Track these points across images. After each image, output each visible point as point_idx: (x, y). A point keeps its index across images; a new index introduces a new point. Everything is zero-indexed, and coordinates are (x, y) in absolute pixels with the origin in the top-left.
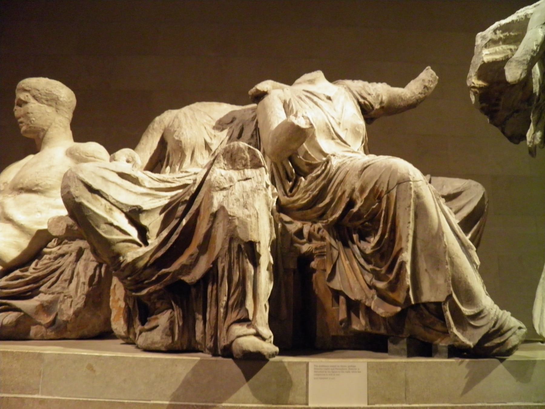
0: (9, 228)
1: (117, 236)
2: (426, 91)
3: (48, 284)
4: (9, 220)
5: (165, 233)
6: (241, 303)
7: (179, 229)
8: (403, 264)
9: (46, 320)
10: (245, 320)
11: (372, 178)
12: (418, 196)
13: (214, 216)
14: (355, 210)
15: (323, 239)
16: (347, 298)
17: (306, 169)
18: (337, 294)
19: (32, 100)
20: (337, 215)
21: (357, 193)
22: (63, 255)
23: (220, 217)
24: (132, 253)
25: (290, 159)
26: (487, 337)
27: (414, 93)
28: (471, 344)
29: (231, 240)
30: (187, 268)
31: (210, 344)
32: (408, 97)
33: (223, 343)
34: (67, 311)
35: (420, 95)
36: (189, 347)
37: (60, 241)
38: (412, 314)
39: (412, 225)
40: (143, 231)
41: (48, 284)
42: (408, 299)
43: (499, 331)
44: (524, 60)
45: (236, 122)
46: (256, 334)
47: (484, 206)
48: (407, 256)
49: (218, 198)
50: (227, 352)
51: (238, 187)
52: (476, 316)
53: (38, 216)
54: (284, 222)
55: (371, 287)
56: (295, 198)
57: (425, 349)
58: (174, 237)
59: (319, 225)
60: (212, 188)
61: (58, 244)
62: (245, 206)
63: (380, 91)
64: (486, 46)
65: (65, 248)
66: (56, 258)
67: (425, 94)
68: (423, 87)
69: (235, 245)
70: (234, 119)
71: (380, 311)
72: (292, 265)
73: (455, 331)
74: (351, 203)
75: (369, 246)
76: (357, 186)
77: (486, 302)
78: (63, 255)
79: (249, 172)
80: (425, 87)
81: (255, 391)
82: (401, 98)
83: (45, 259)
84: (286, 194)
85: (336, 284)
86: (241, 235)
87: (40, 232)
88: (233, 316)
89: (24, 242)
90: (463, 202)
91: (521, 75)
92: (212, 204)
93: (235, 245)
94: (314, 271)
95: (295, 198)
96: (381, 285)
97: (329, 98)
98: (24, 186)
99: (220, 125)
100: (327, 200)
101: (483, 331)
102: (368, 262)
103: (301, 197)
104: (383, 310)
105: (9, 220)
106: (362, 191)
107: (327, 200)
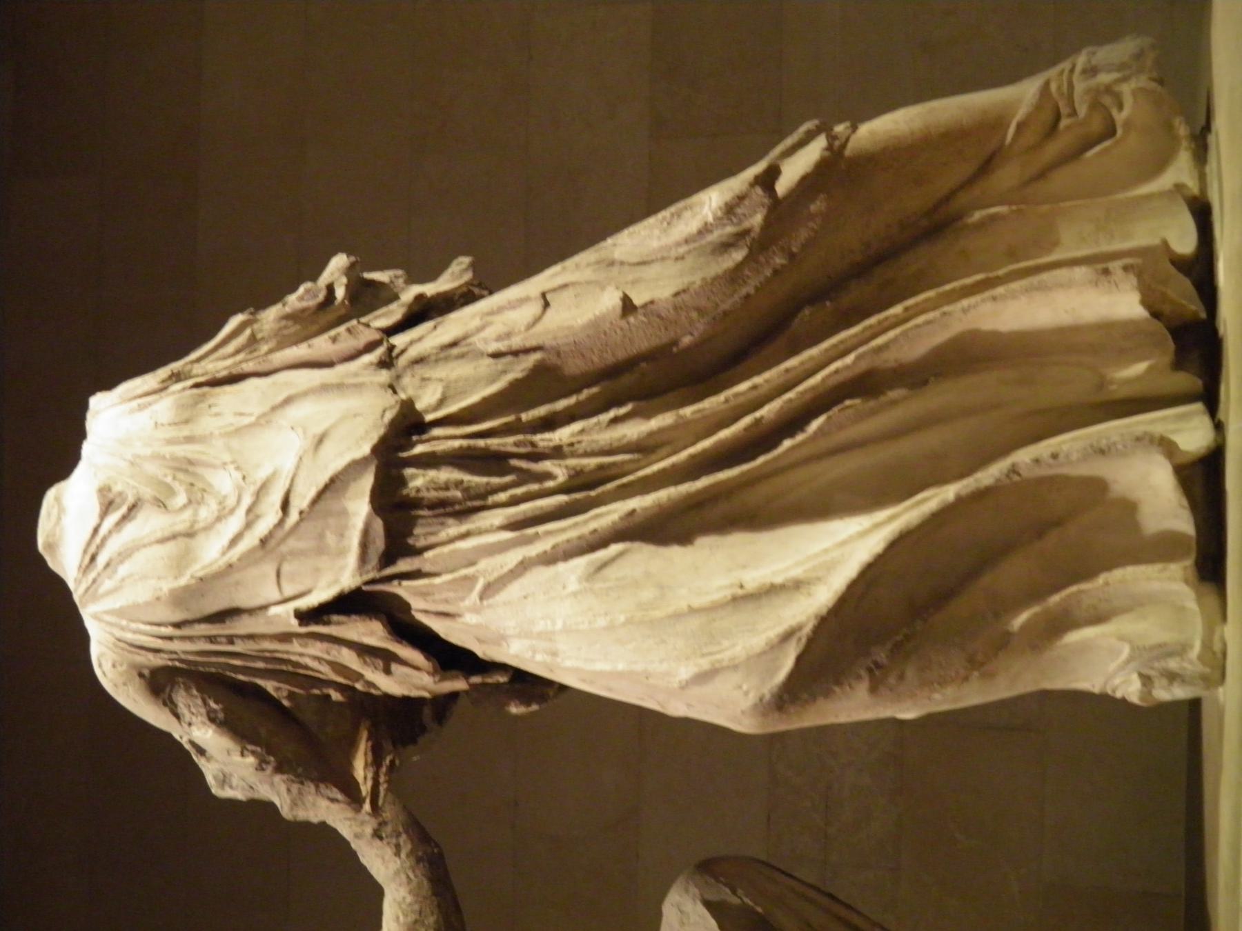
2: (389, 829)
27: (397, 873)
32: (409, 899)
35: (403, 855)
44: (289, 790)
47: (746, 910)
67: (398, 835)
68: (378, 842)
80: (377, 835)
91: (333, 800)
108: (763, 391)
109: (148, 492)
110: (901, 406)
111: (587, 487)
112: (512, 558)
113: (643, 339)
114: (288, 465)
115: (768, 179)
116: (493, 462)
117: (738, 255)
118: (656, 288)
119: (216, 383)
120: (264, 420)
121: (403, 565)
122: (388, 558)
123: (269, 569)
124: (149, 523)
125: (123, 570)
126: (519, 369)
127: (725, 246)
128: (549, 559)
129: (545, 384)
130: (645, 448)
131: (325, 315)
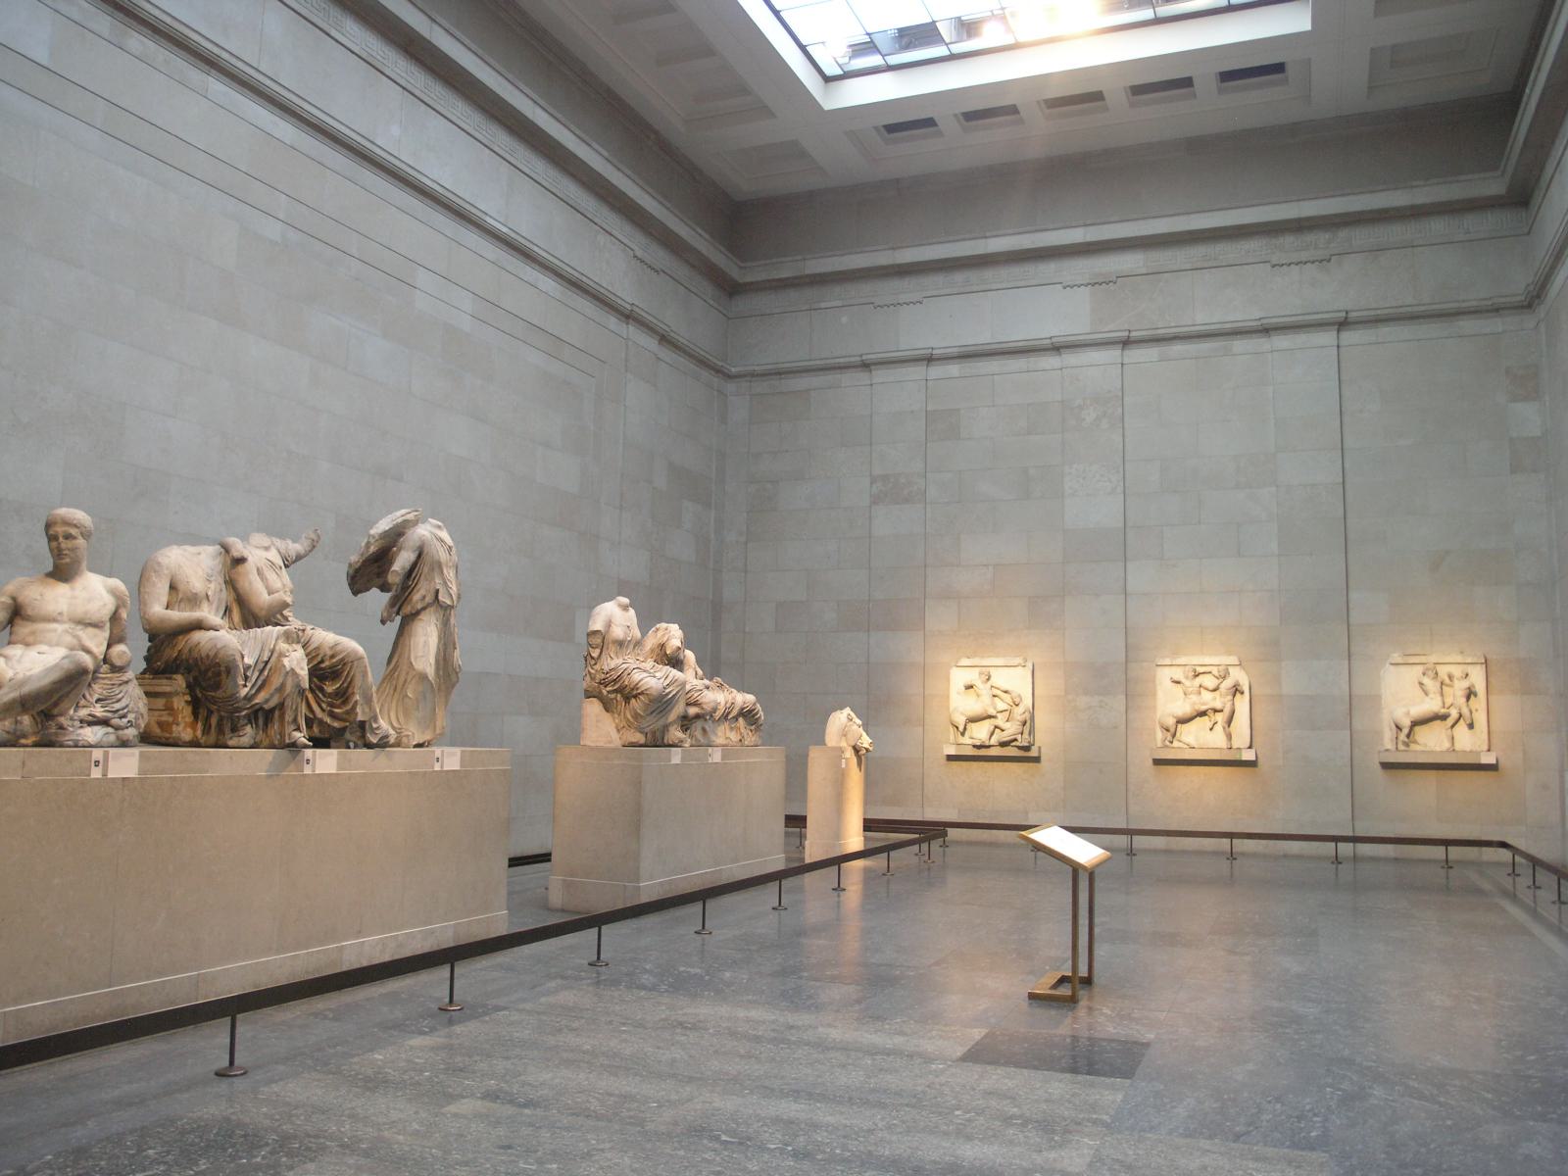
6: (295, 720)
7: (262, 678)
8: (356, 702)
10: (298, 729)
13: (287, 673)
14: (323, 665)
19: (80, 537)
22: (127, 682)
23: (290, 674)
30: (267, 701)
33: (287, 741)
49: (286, 661)
52: (378, 728)
58: (259, 682)
62: (302, 669)
66: (120, 685)
74: (322, 661)
76: (329, 653)
78: (127, 682)
92: (285, 666)
106: (332, 657)
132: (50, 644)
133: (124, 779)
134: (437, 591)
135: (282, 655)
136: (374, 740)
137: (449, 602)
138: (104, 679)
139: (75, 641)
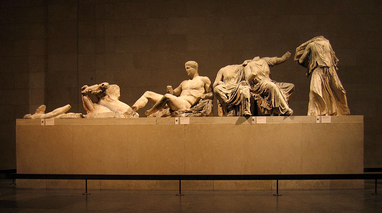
0: (192, 97)
1: (224, 98)
3: (204, 108)
4: (192, 96)
5: (231, 97)
7: (234, 96)
8: (272, 101)
9: (205, 115)
10: (247, 110)
11: (267, 86)
12: (275, 90)
13: (241, 94)
15: (259, 97)
16: (264, 108)
17: (256, 82)
18: (262, 107)
20: (262, 93)
21: (265, 89)
22: (205, 102)
24: (227, 101)
25: (252, 81)
26: (286, 112)
28: (284, 114)
29: (244, 98)
30: (236, 103)
31: (240, 114)
33: (243, 114)
34: (209, 113)
36: (236, 116)
37: (203, 99)
38: (274, 109)
39: (274, 95)
40: (228, 97)
41: (204, 108)
42: (273, 106)
43: (288, 111)
45: (239, 71)
46: (248, 112)
48: (273, 100)
49: (241, 91)
50: (244, 115)
51: (244, 89)
52: (284, 109)
53: (198, 95)
54: (251, 94)
55: (268, 105)
56: (254, 89)
57: (277, 115)
58: (233, 98)
59: (258, 94)
60: (240, 89)
61: (202, 100)
62: (246, 92)
63: (274, 59)
64: (298, 51)
65: (205, 101)
66: (203, 103)
69: (244, 99)
70: (239, 70)
71: (269, 109)
72: (253, 102)
73: (281, 112)
74: (264, 91)
75: (267, 98)
77: (287, 107)
78: (205, 102)
79: (246, 86)
81: (248, 121)
82: (280, 61)
83: (200, 103)
84: (251, 88)
85: (262, 105)
86: (246, 97)
87: (198, 98)
88: (245, 110)
89: (195, 100)
90: (289, 89)
93: (244, 99)
94: (257, 103)
95: (254, 89)
96: (269, 105)
97: (261, 65)
98: (194, 88)
99: (236, 72)
100: (260, 90)
101: (285, 112)
102: (267, 101)
103: (255, 89)
104: (269, 109)
105: (192, 96)
106: (266, 88)
107: (260, 90)
108: (330, 90)
109: (324, 49)
110: (328, 99)
111: (324, 79)
112: (321, 75)
113: (333, 83)
114: (326, 60)
115: (343, 90)
116: (326, 74)
117: (338, 88)
118: (336, 83)
119: (331, 53)
120: (329, 57)
121: (320, 68)
122: (320, 67)
123: (319, 59)
124: (322, 49)
125: (319, 47)
126: (332, 75)
127: (339, 87)
128: (321, 77)
129: (331, 77)
130: (326, 83)
131: (335, 60)
132: (184, 95)
133: (185, 124)
134: (317, 62)
135: (240, 89)
136: (283, 113)
137: (324, 65)
138: (201, 102)
139: (189, 93)
